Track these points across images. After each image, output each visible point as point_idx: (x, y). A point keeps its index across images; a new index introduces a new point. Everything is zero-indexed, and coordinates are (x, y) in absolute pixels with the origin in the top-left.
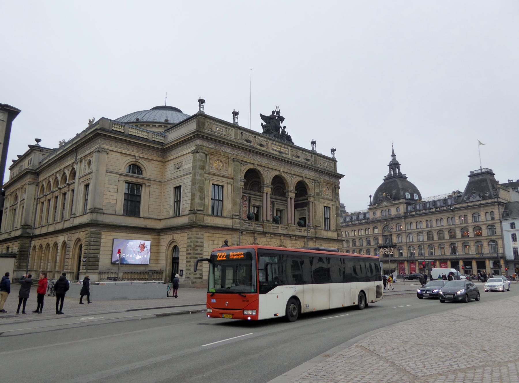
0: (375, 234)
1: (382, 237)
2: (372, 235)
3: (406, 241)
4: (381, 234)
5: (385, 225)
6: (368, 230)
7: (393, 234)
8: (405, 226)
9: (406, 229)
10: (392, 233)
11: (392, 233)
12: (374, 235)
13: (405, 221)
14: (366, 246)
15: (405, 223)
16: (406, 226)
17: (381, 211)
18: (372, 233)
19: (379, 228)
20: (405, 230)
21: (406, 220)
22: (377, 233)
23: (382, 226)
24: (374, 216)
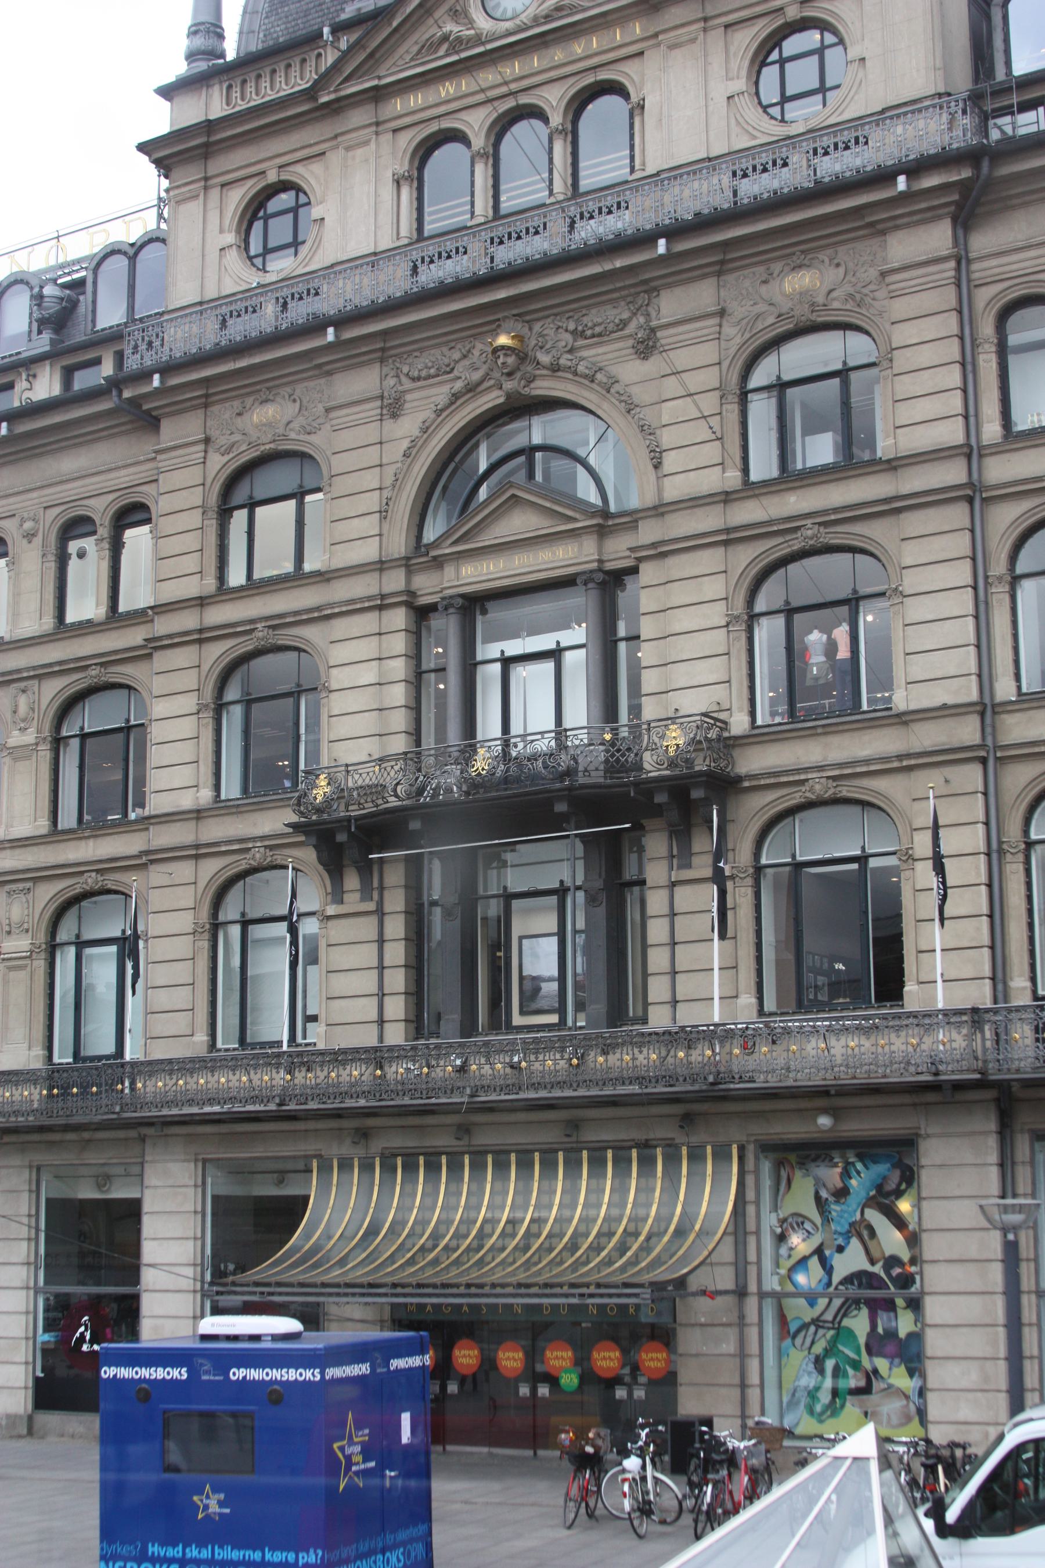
0: (254, 587)
1: (399, 644)
2: (187, 621)
3: (985, 676)
4: (395, 581)
5: (491, 400)
6: (116, 547)
7: (661, 552)
8: (967, 365)
9: (991, 430)
10: (649, 533)
11: (649, 533)
12: (219, 615)
13: (961, 259)
14: (55, 834)
15: (963, 310)
16: (988, 363)
17: (408, 141)
18: (190, 588)
19: (339, 464)
20: (953, 433)
21: (981, 242)
22: (298, 578)
23: (408, 426)
24: (258, 260)
